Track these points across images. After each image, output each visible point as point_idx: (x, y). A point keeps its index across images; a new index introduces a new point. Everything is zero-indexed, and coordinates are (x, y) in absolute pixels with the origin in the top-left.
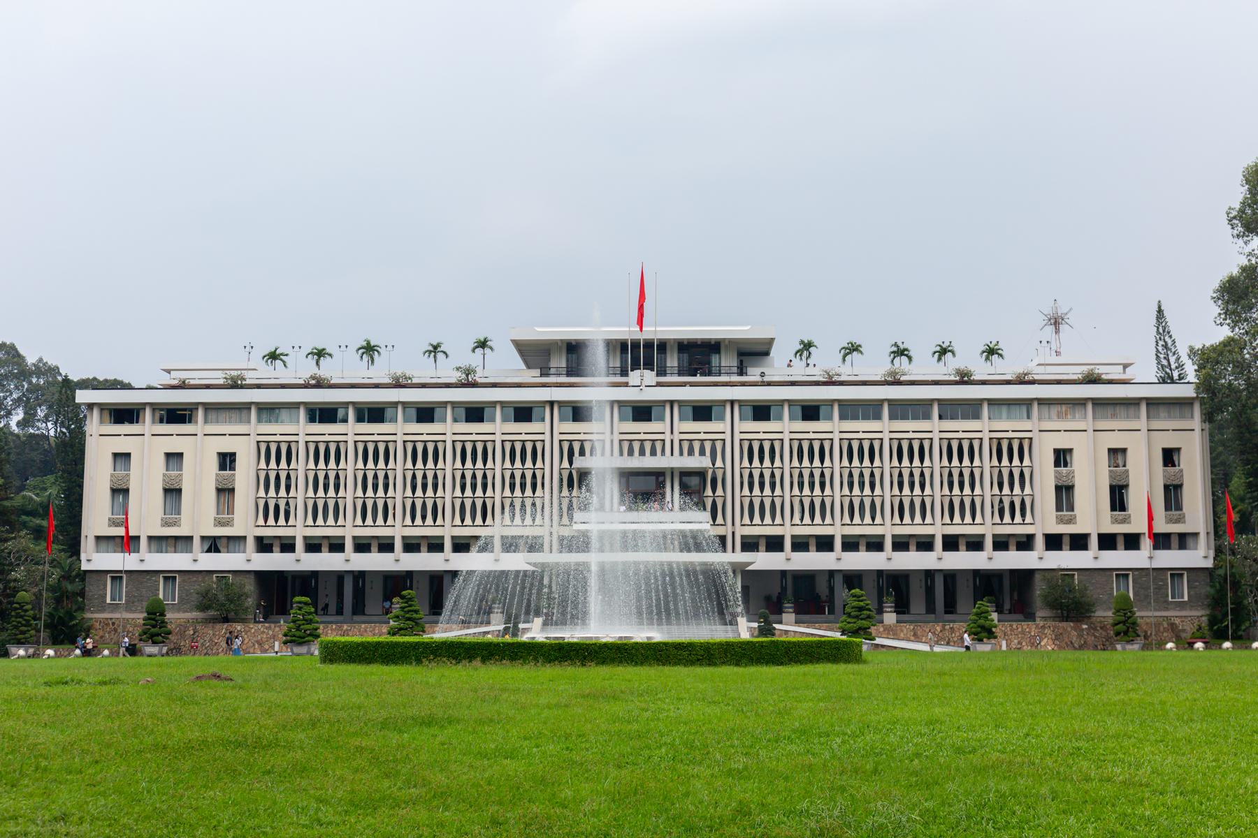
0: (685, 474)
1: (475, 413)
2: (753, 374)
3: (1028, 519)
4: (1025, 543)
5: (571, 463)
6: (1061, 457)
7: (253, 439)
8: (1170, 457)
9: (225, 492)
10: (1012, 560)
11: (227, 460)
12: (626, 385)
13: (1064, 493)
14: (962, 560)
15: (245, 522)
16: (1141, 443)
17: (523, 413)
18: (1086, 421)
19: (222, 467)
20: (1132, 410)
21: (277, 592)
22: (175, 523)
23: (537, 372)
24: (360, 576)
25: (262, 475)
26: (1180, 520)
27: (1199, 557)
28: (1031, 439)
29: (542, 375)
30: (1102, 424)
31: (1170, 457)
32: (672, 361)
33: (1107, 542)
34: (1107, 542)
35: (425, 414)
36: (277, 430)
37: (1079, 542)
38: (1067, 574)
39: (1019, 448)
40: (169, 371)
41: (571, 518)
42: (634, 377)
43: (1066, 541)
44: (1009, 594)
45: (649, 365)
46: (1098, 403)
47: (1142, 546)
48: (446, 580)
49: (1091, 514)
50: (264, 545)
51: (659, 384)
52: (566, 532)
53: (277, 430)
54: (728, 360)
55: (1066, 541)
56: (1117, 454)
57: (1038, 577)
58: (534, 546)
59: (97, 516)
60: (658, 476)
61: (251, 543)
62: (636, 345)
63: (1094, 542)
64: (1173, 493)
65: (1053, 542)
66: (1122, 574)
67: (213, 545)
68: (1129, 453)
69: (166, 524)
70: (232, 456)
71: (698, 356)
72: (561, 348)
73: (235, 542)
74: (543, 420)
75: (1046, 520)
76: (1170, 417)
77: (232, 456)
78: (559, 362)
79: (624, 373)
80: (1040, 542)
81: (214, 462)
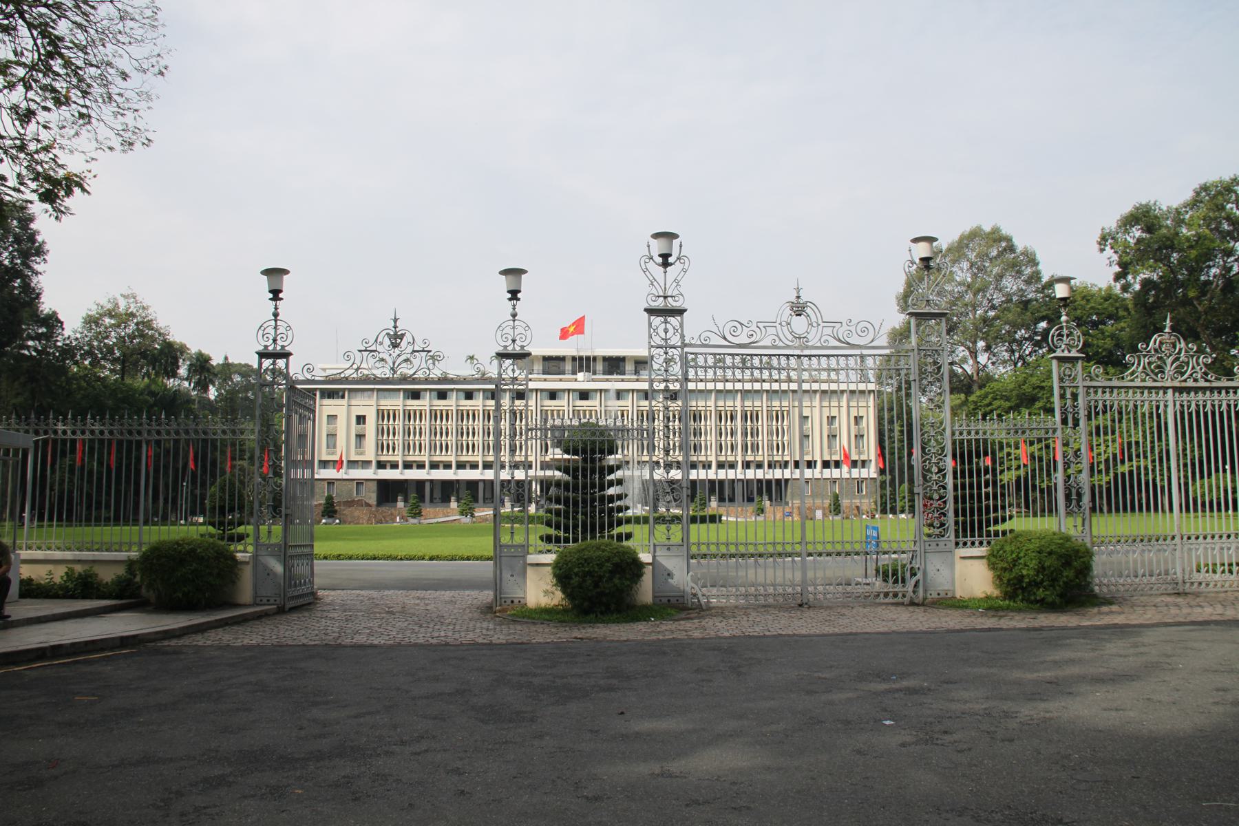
2: (644, 374)
9: (361, 437)
10: (778, 474)
11: (361, 419)
13: (805, 437)
14: (750, 474)
15: (370, 453)
19: (358, 423)
21: (388, 491)
32: (600, 366)
33: (826, 464)
36: (389, 403)
40: (324, 370)
42: (580, 376)
44: (774, 490)
45: (588, 370)
48: (481, 486)
50: (381, 465)
51: (593, 380)
53: (389, 403)
54: (629, 367)
61: (374, 464)
62: (581, 358)
66: (834, 481)
67: (353, 464)
70: (364, 417)
71: (614, 365)
73: (366, 464)
77: (364, 417)
79: (574, 373)
81: (354, 420)
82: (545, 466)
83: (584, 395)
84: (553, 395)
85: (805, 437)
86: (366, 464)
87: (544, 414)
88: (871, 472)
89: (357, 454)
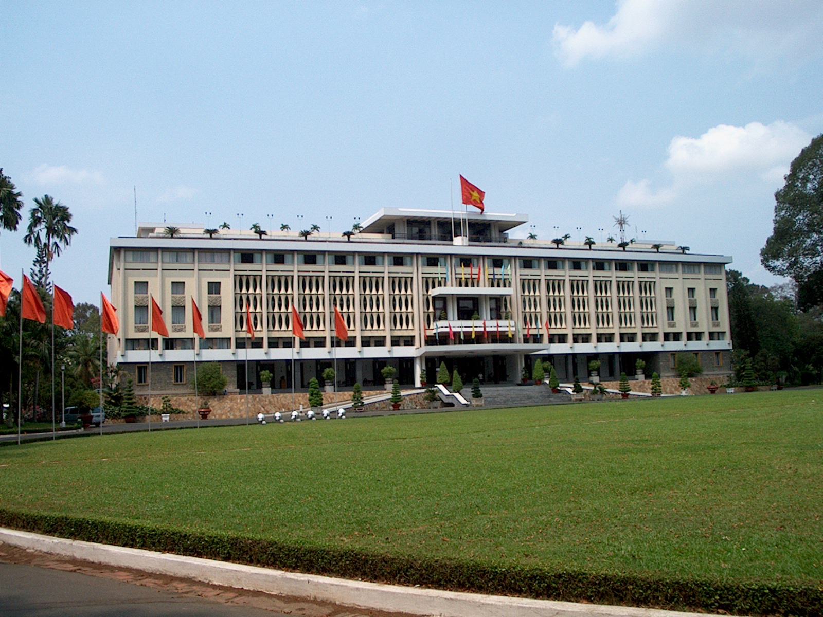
0: (492, 298)
1: (370, 259)
3: (655, 325)
4: (653, 337)
5: (427, 291)
6: (669, 290)
7: (232, 273)
8: (713, 291)
9: (215, 309)
11: (214, 288)
12: (452, 245)
15: (228, 329)
16: (702, 283)
17: (398, 260)
18: (679, 274)
20: (696, 269)
22: (180, 330)
23: (390, 236)
24: (302, 363)
25: (239, 296)
26: (718, 325)
27: (725, 344)
28: (655, 282)
29: (393, 238)
30: (686, 276)
31: (713, 291)
33: (690, 336)
34: (690, 336)
35: (340, 258)
37: (677, 337)
38: (673, 353)
39: (646, 287)
41: (429, 325)
42: (458, 241)
43: (671, 336)
46: (684, 264)
47: (703, 339)
49: (682, 324)
50: (241, 344)
51: (469, 246)
52: (430, 333)
54: (495, 233)
55: (671, 336)
56: (691, 291)
57: (661, 355)
58: (409, 341)
59: (126, 324)
60: (475, 300)
63: (684, 336)
64: (715, 309)
65: (667, 337)
66: (696, 352)
68: (696, 292)
69: (175, 330)
70: (219, 284)
71: (481, 230)
72: (404, 221)
74: (412, 264)
75: (661, 326)
76: (711, 273)
77: (219, 284)
78: (401, 229)
80: (661, 337)
82: (430, 341)
83: (466, 261)
84: (432, 260)
85: (671, 309)
86: (224, 342)
87: (429, 283)
88: (725, 344)
89: (213, 329)
